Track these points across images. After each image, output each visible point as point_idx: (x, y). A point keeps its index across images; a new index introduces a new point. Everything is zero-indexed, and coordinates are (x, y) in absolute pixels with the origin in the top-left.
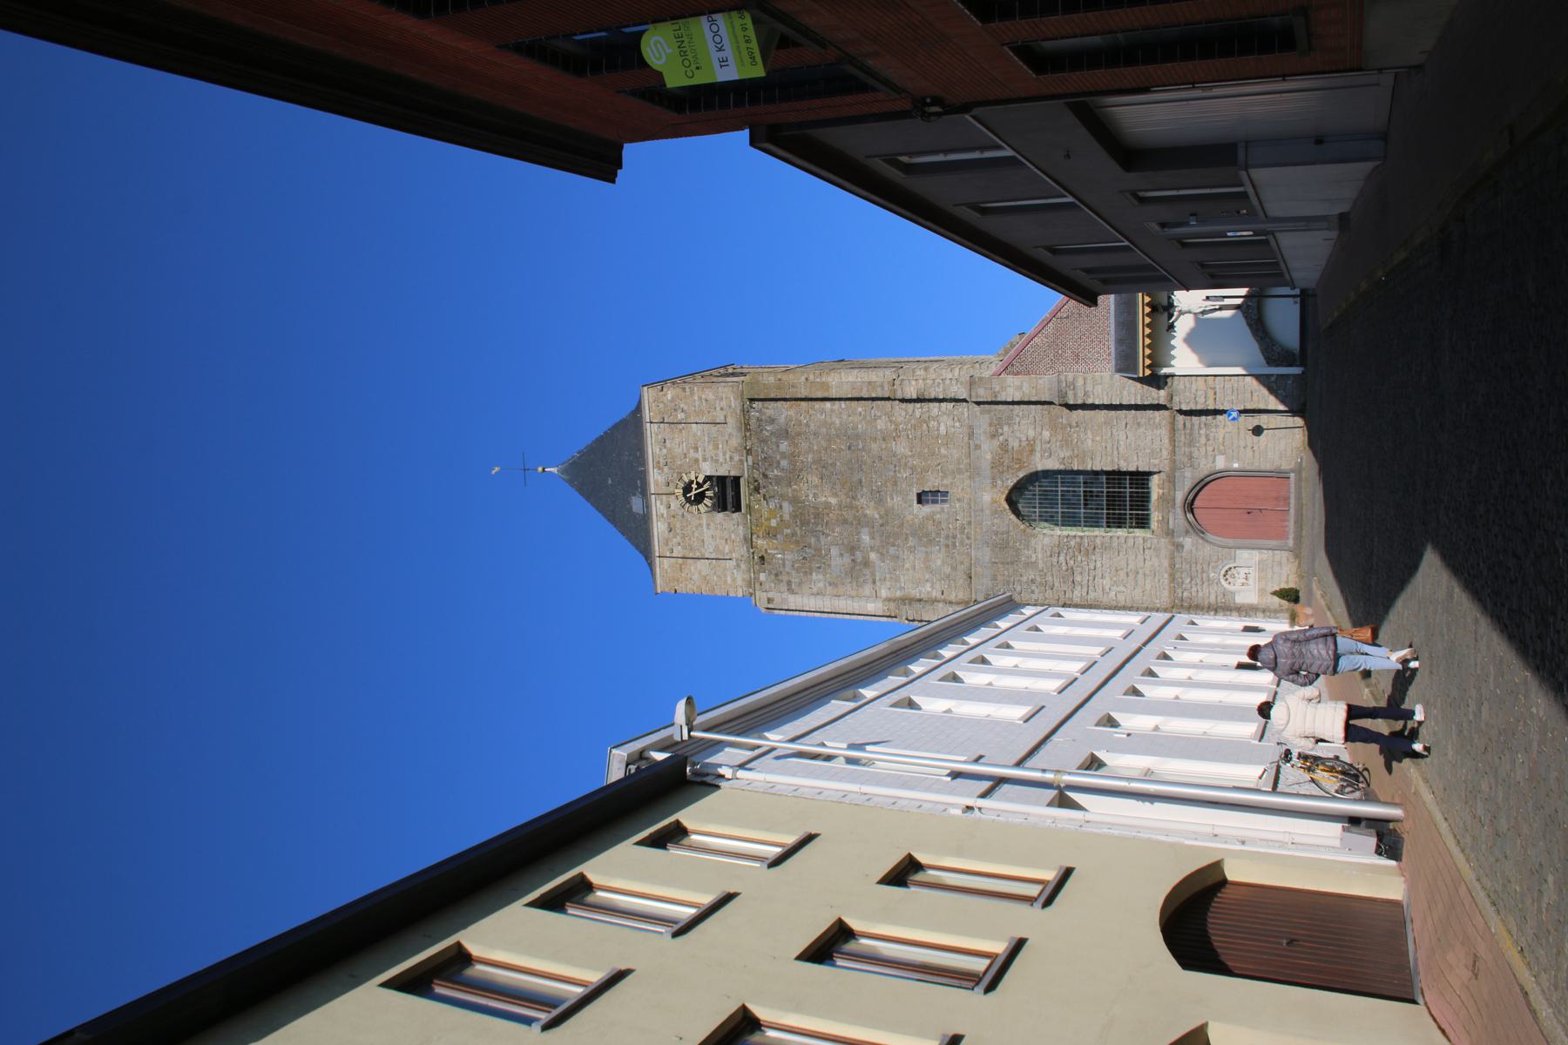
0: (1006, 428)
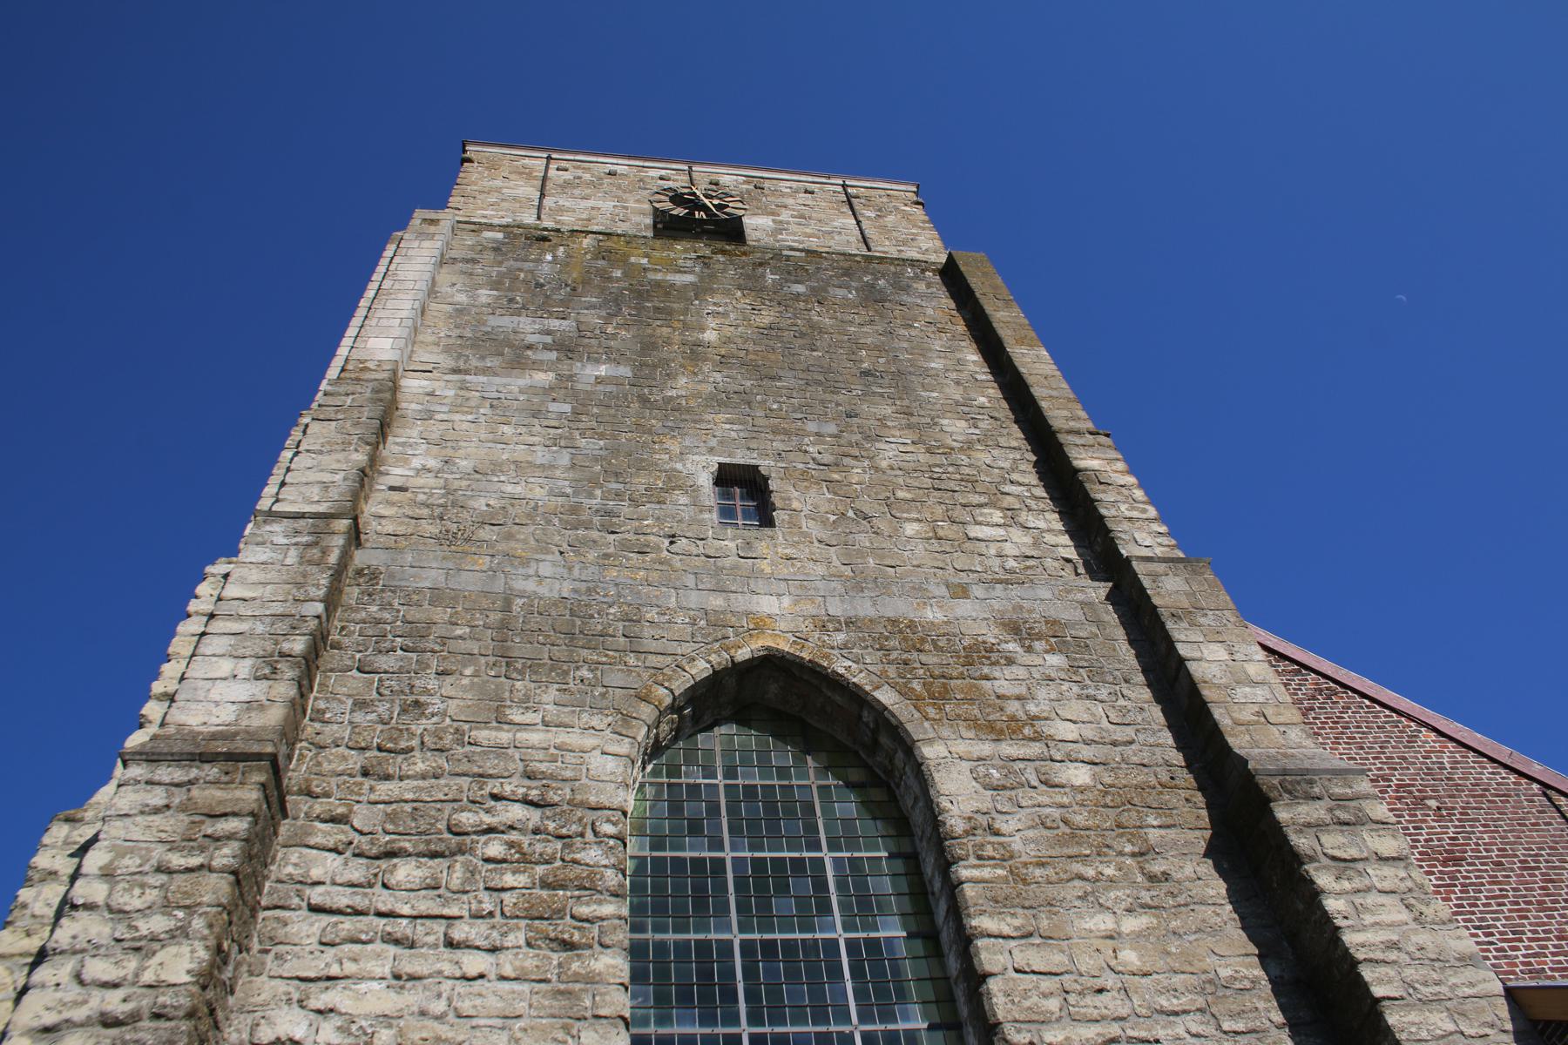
0: (1055, 660)
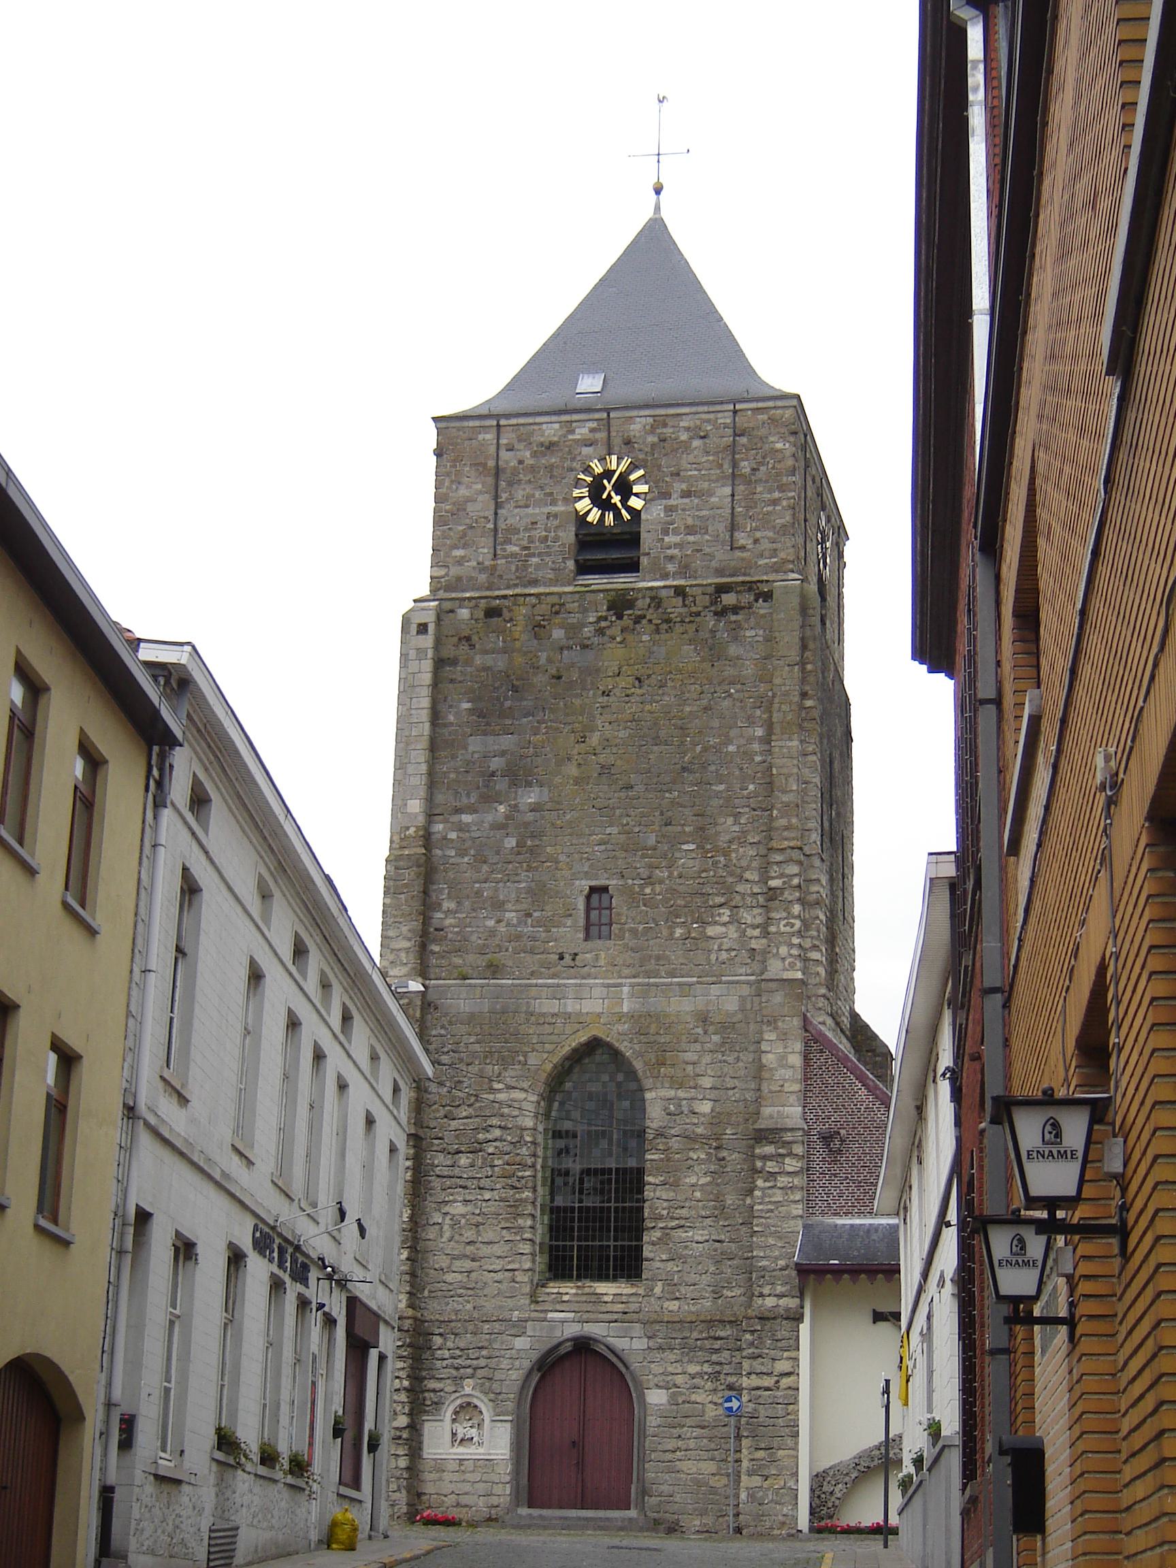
0: (716, 1038)
